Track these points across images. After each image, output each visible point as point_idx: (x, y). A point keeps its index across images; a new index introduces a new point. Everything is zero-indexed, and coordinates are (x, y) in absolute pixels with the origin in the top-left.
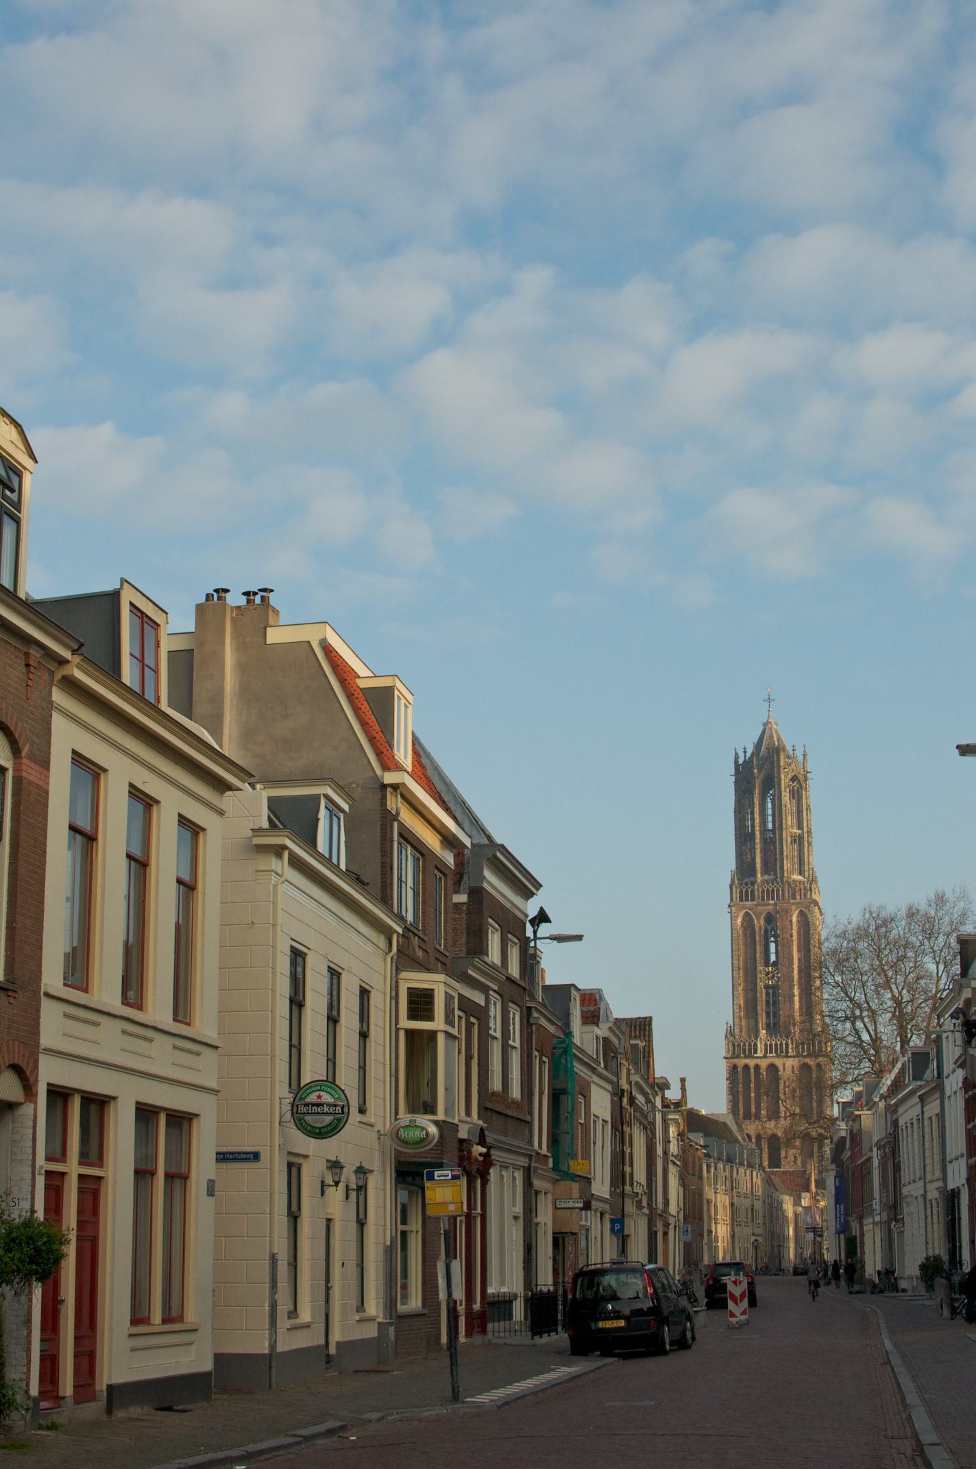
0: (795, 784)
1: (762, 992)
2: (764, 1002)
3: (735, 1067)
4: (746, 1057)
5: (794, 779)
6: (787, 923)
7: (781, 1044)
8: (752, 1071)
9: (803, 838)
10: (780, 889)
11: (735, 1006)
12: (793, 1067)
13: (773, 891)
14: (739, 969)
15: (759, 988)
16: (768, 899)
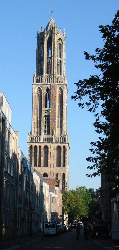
0: (60, 41)
1: (43, 118)
2: (44, 122)
3: (31, 146)
4: (35, 143)
5: (60, 39)
6: (54, 91)
7: (50, 138)
8: (38, 148)
9: (62, 61)
10: (52, 79)
11: (33, 123)
12: (54, 147)
13: (49, 80)
14: (35, 109)
15: (42, 116)
16: (48, 83)
